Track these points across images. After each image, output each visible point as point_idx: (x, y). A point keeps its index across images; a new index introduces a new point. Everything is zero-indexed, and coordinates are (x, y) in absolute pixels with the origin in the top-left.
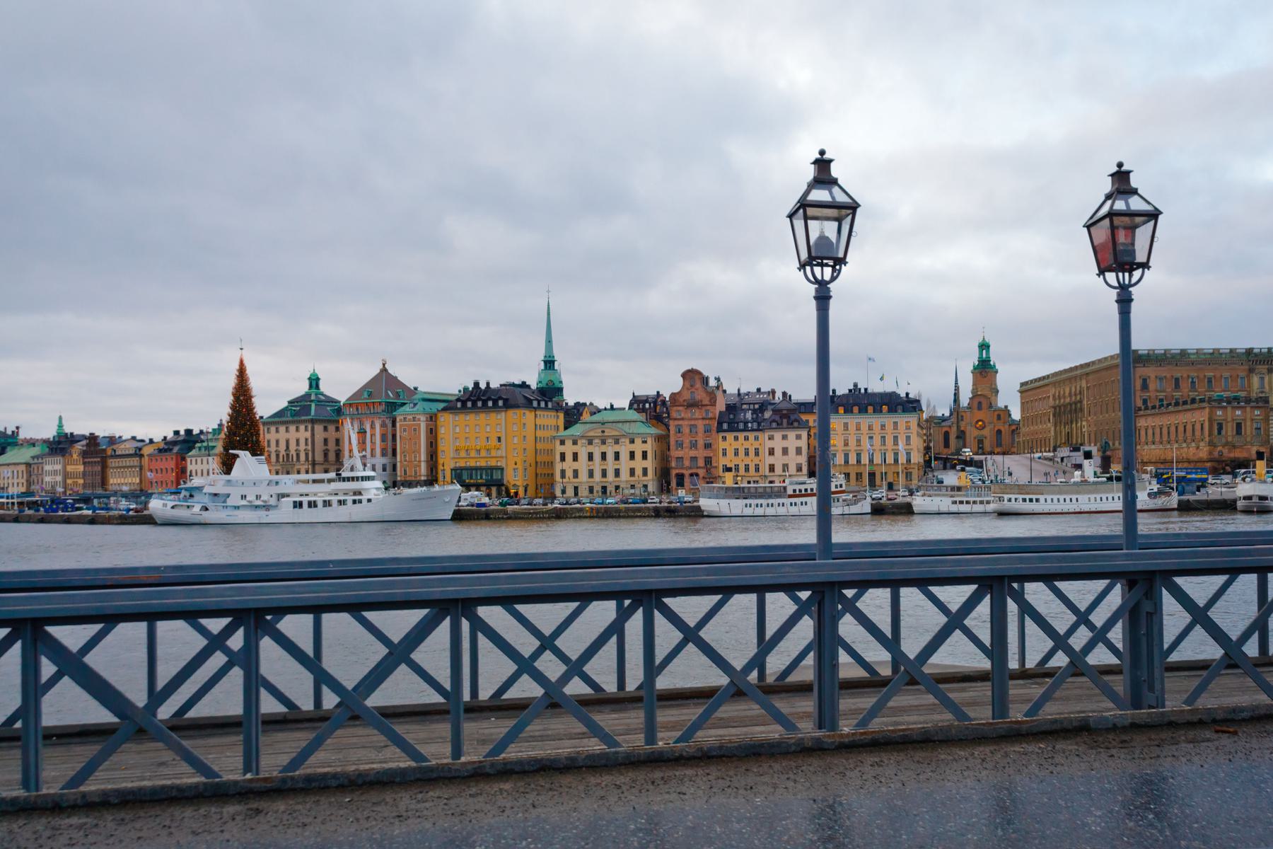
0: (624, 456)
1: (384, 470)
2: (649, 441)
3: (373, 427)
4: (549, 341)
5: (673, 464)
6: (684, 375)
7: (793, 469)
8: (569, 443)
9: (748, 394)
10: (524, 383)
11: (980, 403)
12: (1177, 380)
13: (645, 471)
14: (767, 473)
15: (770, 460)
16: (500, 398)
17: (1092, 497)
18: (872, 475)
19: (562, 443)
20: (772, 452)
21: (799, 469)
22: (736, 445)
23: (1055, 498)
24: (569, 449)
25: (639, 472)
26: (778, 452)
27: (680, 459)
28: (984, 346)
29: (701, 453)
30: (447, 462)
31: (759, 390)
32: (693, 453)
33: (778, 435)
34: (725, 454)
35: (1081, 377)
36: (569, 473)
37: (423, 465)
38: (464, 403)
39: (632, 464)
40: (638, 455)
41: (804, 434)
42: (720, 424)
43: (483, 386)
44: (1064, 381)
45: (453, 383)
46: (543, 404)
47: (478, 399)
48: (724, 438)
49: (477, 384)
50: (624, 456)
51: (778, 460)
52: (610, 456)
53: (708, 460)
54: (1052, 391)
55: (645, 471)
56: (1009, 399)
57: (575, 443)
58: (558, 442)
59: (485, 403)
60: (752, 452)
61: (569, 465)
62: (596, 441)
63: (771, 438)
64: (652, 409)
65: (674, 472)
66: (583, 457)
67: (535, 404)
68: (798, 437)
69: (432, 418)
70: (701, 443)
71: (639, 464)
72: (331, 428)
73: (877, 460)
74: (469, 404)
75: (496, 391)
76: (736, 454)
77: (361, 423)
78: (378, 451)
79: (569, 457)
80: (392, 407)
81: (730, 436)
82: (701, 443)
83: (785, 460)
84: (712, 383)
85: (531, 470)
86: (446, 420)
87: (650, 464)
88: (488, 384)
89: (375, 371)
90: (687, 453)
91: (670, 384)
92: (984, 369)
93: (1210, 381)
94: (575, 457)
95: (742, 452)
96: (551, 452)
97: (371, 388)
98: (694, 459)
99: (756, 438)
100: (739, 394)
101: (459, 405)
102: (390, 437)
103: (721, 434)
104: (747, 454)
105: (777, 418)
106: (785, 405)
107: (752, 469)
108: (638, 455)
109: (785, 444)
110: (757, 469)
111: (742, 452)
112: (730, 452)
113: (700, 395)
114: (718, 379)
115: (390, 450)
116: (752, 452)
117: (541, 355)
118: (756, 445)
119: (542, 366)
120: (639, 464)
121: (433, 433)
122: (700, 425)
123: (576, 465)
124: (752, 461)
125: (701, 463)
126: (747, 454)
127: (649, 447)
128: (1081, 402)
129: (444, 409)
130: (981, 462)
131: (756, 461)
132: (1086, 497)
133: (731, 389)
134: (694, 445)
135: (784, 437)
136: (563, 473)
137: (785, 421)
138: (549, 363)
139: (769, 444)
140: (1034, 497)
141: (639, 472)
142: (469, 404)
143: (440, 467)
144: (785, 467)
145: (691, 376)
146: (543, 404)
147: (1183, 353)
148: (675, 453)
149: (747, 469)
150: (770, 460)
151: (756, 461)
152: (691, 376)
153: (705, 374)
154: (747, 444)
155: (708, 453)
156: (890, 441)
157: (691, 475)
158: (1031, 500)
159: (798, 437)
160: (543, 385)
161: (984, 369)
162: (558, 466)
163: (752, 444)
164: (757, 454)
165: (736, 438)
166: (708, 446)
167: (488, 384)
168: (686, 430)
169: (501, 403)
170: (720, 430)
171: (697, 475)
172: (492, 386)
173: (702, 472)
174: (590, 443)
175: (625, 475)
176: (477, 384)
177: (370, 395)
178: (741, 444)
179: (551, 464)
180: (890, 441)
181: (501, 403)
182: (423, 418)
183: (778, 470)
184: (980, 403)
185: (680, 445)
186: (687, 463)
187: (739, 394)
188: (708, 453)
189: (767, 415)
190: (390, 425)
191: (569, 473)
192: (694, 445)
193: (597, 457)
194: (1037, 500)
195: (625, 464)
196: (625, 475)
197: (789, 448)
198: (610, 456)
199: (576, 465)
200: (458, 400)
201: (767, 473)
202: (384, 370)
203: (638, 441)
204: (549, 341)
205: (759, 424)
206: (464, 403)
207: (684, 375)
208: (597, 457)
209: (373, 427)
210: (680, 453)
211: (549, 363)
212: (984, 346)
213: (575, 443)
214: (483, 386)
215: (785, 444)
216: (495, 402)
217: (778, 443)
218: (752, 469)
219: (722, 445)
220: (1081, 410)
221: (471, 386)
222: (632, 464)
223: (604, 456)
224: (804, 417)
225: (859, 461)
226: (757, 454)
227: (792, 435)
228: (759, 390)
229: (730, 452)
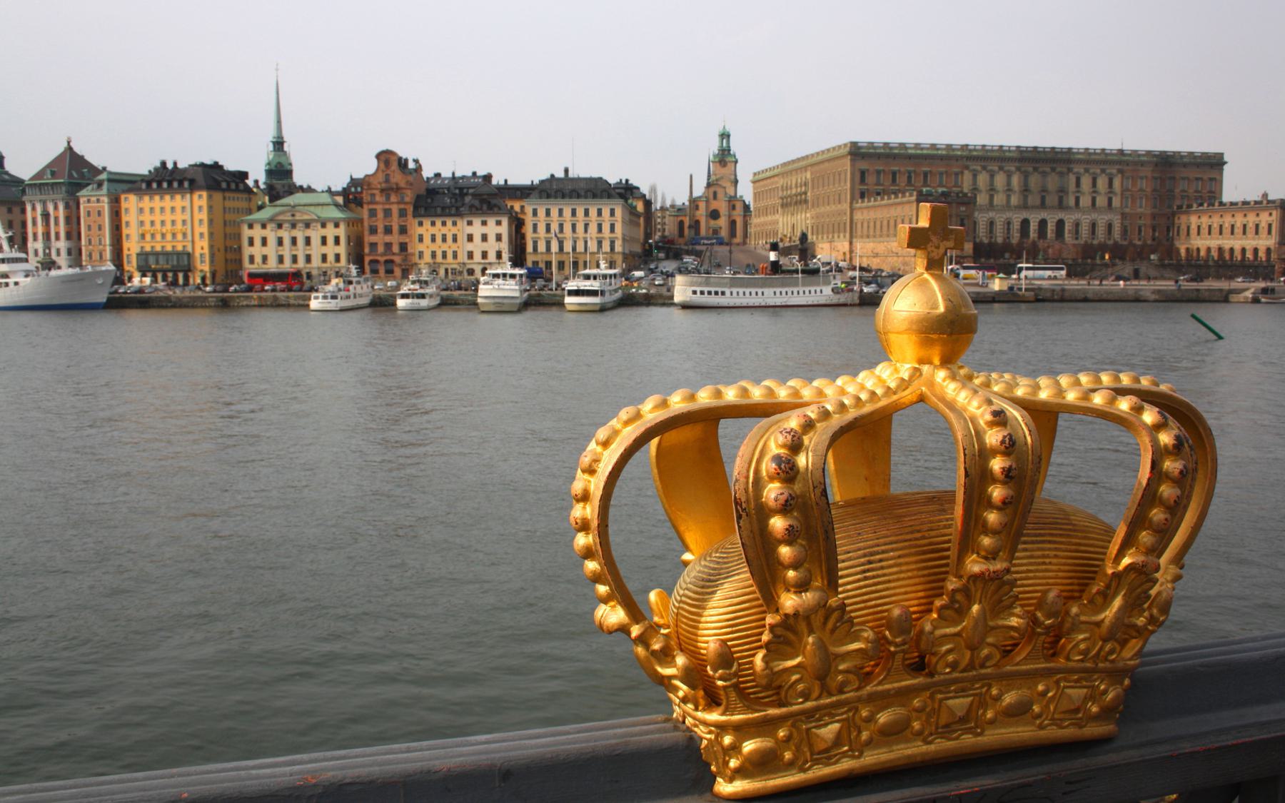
0: (316, 241)
1: (69, 253)
2: (342, 226)
3: (56, 208)
4: (279, 122)
5: (367, 250)
6: (378, 156)
7: (492, 257)
8: (257, 227)
9: (463, 177)
10: (216, 163)
11: (715, 193)
12: (894, 174)
13: (337, 258)
14: (466, 261)
15: (470, 247)
16: (185, 179)
17: (778, 290)
18: (576, 264)
19: (251, 226)
20: (470, 238)
21: (499, 255)
22: (433, 230)
23: (753, 291)
24: (257, 233)
25: (331, 258)
26: (477, 238)
27: (373, 246)
28: (725, 136)
29: (395, 239)
30: (132, 247)
31: (474, 174)
32: (388, 239)
33: (477, 222)
34: (421, 239)
35: (805, 168)
36: (258, 259)
37: (108, 249)
38: (149, 184)
39: (324, 250)
40: (330, 241)
41: (505, 221)
42: (416, 208)
43: (170, 166)
44: (791, 172)
45: (143, 166)
46: (233, 186)
47: (167, 179)
48: (421, 224)
49: (164, 164)
50: (316, 241)
51: (477, 247)
52: (301, 242)
53: (403, 247)
54: (781, 182)
55: (337, 258)
56: (746, 191)
57: (264, 226)
58: (245, 227)
59: (170, 184)
60: (450, 238)
61: (257, 250)
62: (286, 225)
63: (470, 223)
64: (353, 195)
65: (367, 259)
66: (272, 241)
67: (224, 185)
68: (499, 223)
69: (115, 202)
70: (396, 228)
71: (330, 250)
72: (16, 210)
73: (580, 248)
74: (155, 185)
75: (185, 170)
76: (433, 239)
77: (44, 203)
78: (62, 235)
79: (258, 242)
80: (75, 187)
81: (427, 222)
82: (396, 228)
83: (485, 246)
84: (411, 165)
85: (220, 256)
86: (130, 203)
87: (342, 249)
88: (175, 164)
89: (60, 148)
90: (380, 238)
91: (366, 166)
92: (724, 157)
93: (894, 174)
94: (264, 242)
95: (439, 239)
96: (238, 237)
97: (53, 167)
98: (388, 246)
99: (455, 224)
100: (454, 177)
101: (144, 186)
102: (75, 220)
103: (417, 221)
104: (444, 239)
105: (477, 203)
106: (485, 190)
107: (450, 255)
108: (330, 241)
109: (484, 230)
110: (455, 255)
111: (439, 239)
112: (427, 239)
113: (397, 178)
114: (416, 161)
115: (75, 234)
116: (450, 238)
117: (270, 135)
118: (454, 230)
119: (271, 147)
120: (330, 250)
121: (116, 214)
122: (395, 209)
123: (265, 251)
124: (449, 247)
125: (396, 249)
126: (444, 239)
127: (342, 232)
128: (805, 193)
129: (129, 191)
130: (701, 252)
131: (454, 247)
132: (772, 290)
133: (427, 173)
134: (388, 230)
135: (484, 223)
136: (252, 259)
137: (485, 207)
138: (279, 144)
139: (469, 230)
140: (720, 290)
141: (331, 258)
142: (155, 185)
143: (126, 252)
144: (485, 255)
145: (385, 157)
146: (233, 186)
147: (902, 146)
148: (368, 239)
149: (444, 255)
150: (470, 247)
151: (454, 247)
152: (385, 157)
153: (403, 154)
154: (444, 230)
155: (404, 239)
156: (606, 228)
157: (386, 262)
158: (716, 293)
159: (499, 223)
160: (273, 167)
161: (724, 157)
162: (247, 251)
163: (449, 230)
164: (455, 239)
165: (433, 224)
166: (403, 230)
167: (175, 164)
168: (380, 215)
169: (186, 184)
170: (416, 214)
171: (392, 261)
172: (180, 166)
173: (397, 259)
174: (280, 226)
175: (316, 262)
176: (164, 164)
177: (53, 174)
178: (438, 230)
179: (239, 250)
180: (606, 228)
181: (186, 184)
182: (106, 199)
183: (477, 257)
184: (715, 193)
185: (373, 231)
186: (381, 249)
187: (454, 177)
188: (404, 239)
189: (468, 199)
190: (74, 207)
191: (258, 259)
192: (388, 230)
193: (287, 241)
194: (723, 293)
195: (316, 250)
196: (316, 262)
197: (484, 236)
198: (301, 242)
199: (265, 251)
200: (142, 181)
201: (466, 261)
202: (70, 149)
203: (330, 226)
204: (279, 122)
205: (457, 208)
206: (149, 184)
207: (378, 156)
208: (287, 241)
209: (56, 208)
210: (373, 239)
211: (279, 144)
212: (725, 136)
213: (264, 226)
214: (170, 166)
215: (484, 230)
216: (181, 183)
217: (477, 229)
218: (450, 255)
219: (420, 230)
220: (806, 201)
221: (158, 165)
222: (324, 250)
223: (308, 241)
224: (509, 204)
225: (561, 248)
226: (455, 239)
227: (491, 221)
228: (474, 174)
229: (427, 239)
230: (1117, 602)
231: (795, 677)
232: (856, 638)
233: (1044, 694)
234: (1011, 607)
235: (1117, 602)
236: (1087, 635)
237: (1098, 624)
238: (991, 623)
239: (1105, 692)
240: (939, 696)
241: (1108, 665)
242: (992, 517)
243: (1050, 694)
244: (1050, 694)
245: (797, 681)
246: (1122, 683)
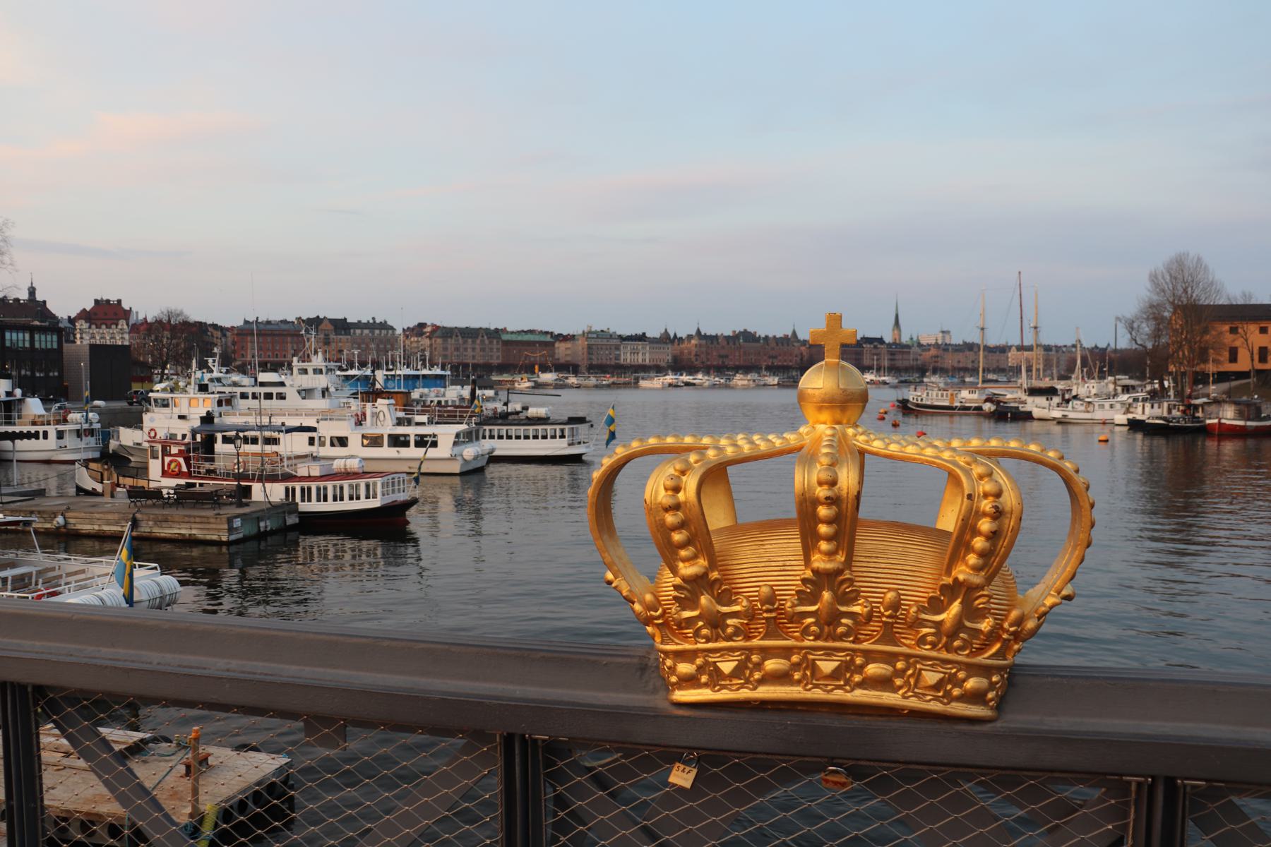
230: (955, 607)
231: (701, 623)
232: (735, 602)
233: (904, 671)
234: (856, 599)
235: (955, 607)
236: (932, 630)
237: (941, 623)
238: (843, 609)
239: (964, 680)
240: (811, 657)
241: (960, 658)
242: (823, 529)
243: (910, 672)
244: (910, 672)
245: (700, 628)
246: (989, 678)
